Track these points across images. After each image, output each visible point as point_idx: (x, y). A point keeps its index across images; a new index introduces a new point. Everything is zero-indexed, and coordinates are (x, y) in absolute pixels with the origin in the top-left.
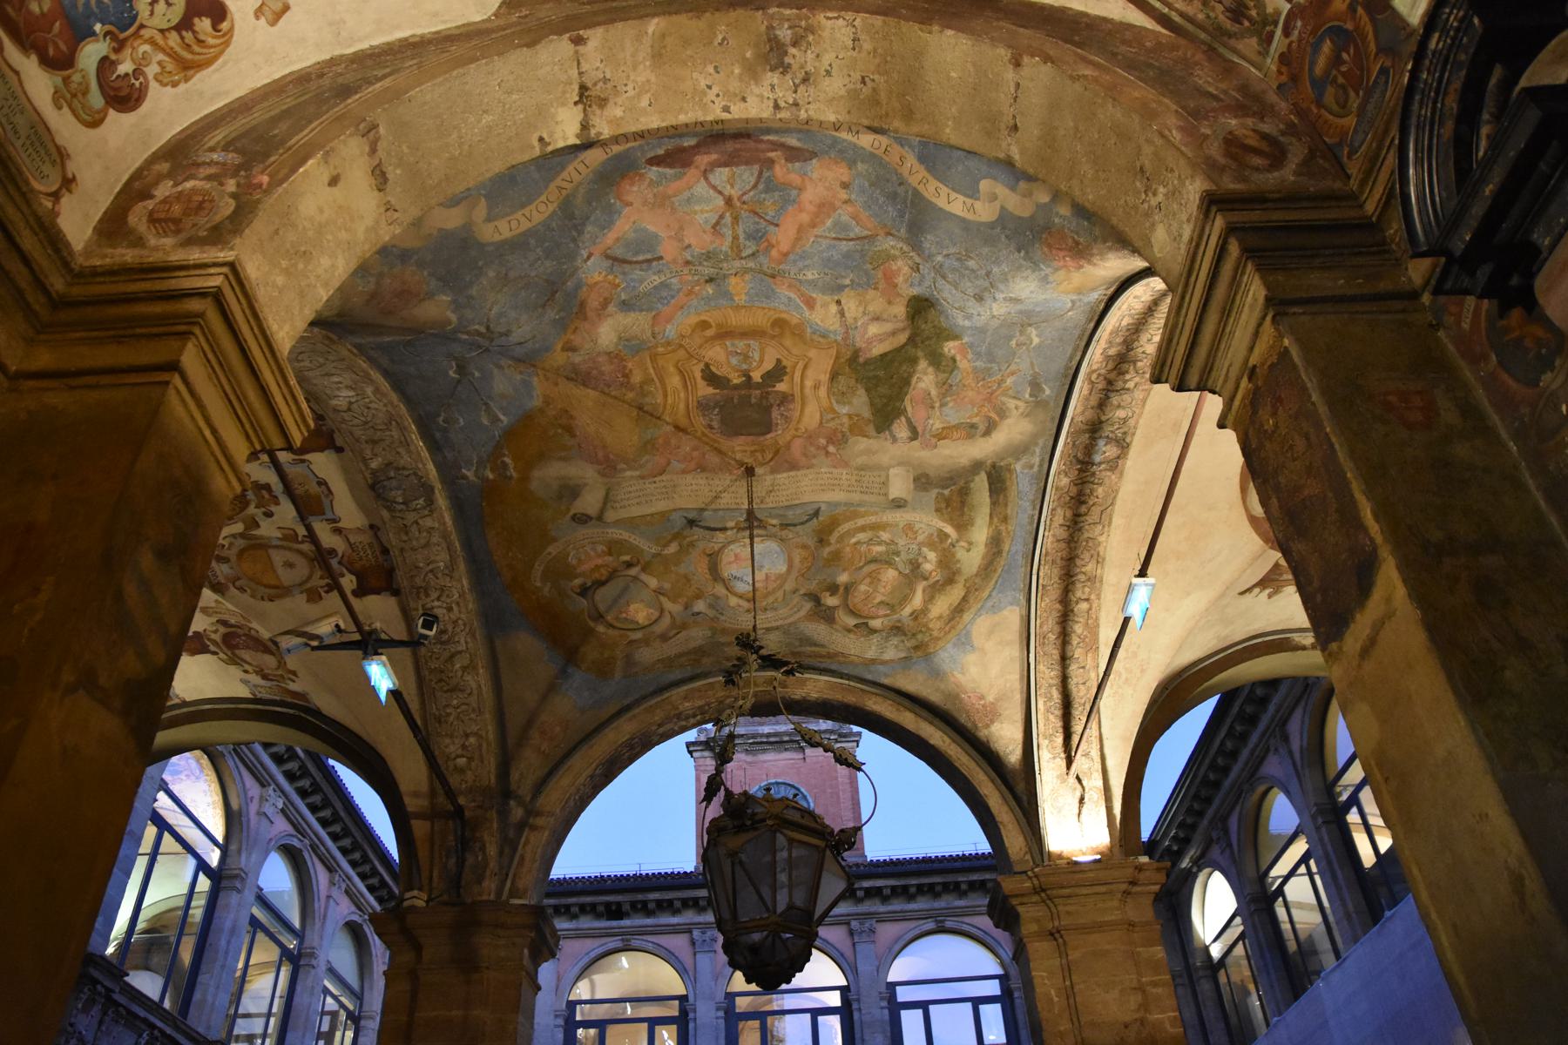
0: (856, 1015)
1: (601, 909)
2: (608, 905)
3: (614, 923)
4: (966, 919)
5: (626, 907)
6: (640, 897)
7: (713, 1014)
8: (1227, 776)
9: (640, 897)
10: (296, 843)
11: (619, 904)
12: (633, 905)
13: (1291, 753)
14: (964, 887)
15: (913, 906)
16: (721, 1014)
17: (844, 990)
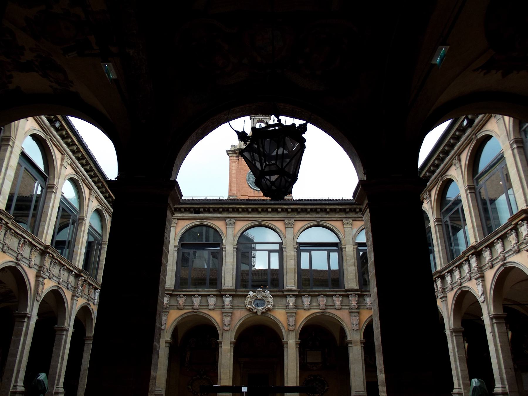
0: (284, 253)
1: (192, 210)
2: (195, 209)
3: (197, 215)
4: (328, 222)
5: (202, 210)
6: (207, 206)
7: (232, 249)
8: (438, 168)
9: (207, 206)
10: (76, 177)
11: (199, 209)
12: (204, 209)
13: (461, 166)
14: (328, 210)
15: (308, 216)
16: (235, 250)
17: (281, 244)
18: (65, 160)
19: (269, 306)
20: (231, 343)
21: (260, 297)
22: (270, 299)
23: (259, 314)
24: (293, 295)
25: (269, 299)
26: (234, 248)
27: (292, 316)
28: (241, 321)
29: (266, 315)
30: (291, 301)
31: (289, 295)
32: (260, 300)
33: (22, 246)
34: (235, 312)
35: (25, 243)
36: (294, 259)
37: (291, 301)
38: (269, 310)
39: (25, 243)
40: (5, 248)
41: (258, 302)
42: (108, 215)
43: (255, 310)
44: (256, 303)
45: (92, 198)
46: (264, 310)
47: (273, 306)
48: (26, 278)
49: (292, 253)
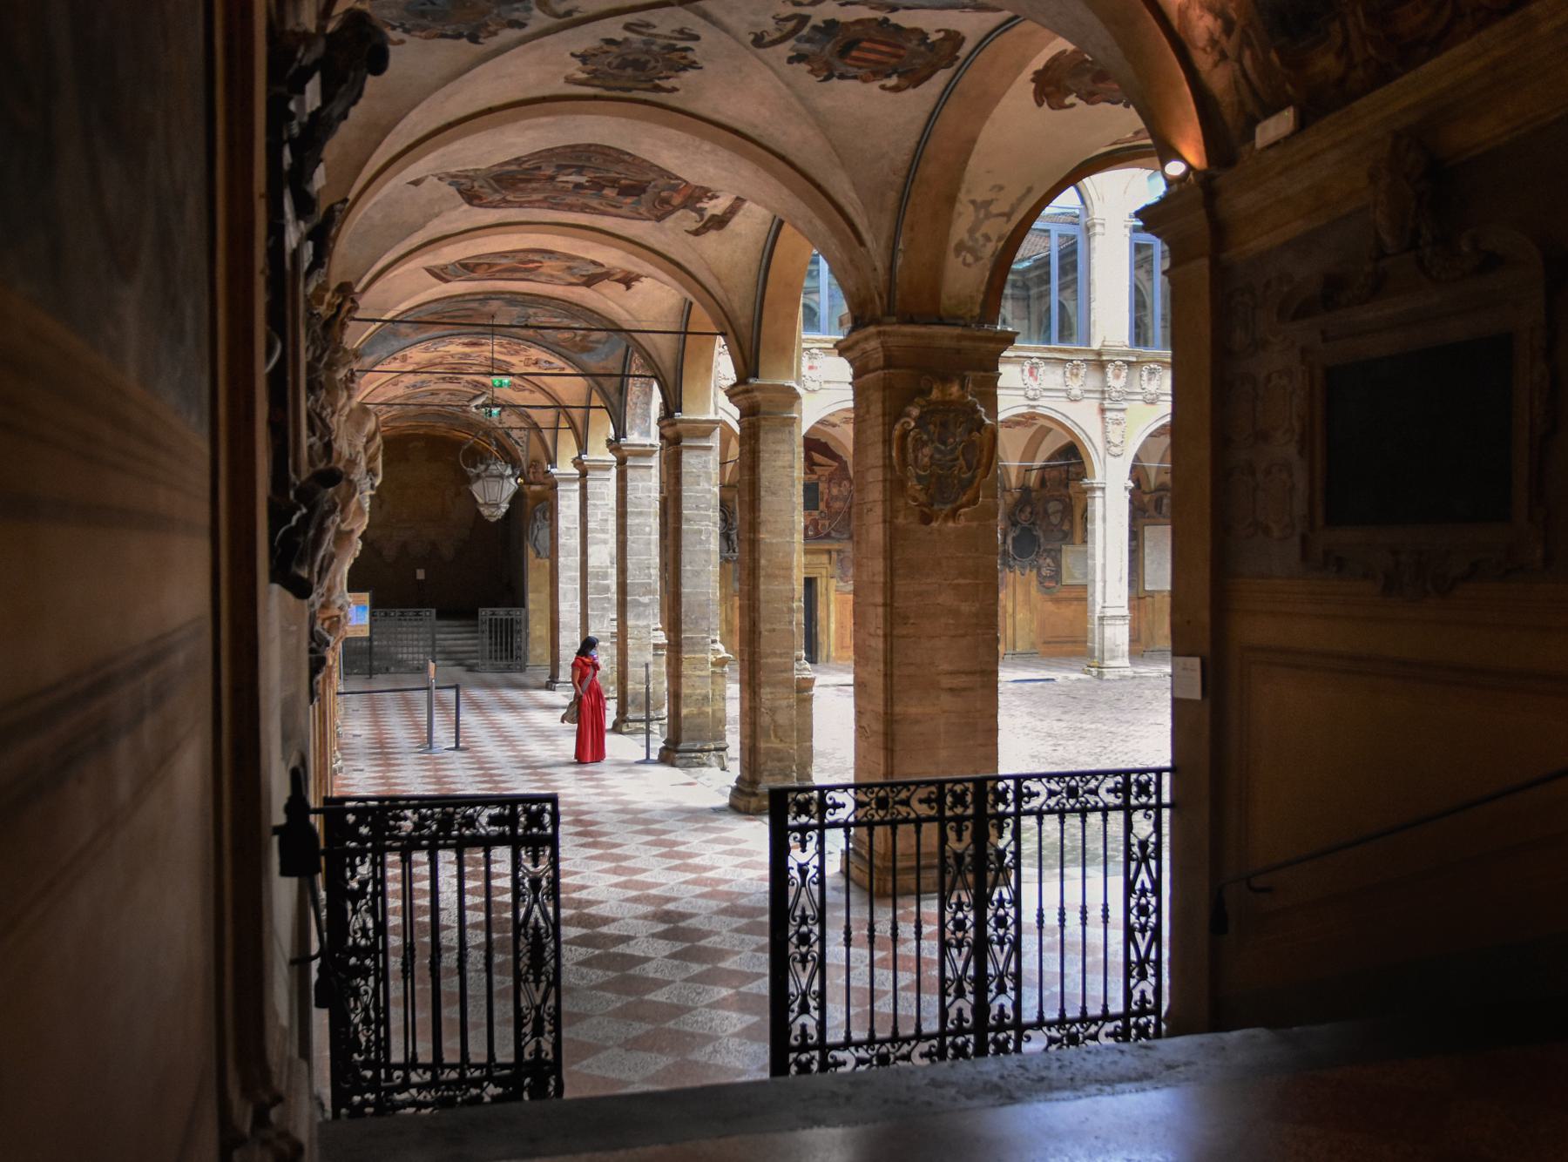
33: (1031, 374)
48: (1068, 423)
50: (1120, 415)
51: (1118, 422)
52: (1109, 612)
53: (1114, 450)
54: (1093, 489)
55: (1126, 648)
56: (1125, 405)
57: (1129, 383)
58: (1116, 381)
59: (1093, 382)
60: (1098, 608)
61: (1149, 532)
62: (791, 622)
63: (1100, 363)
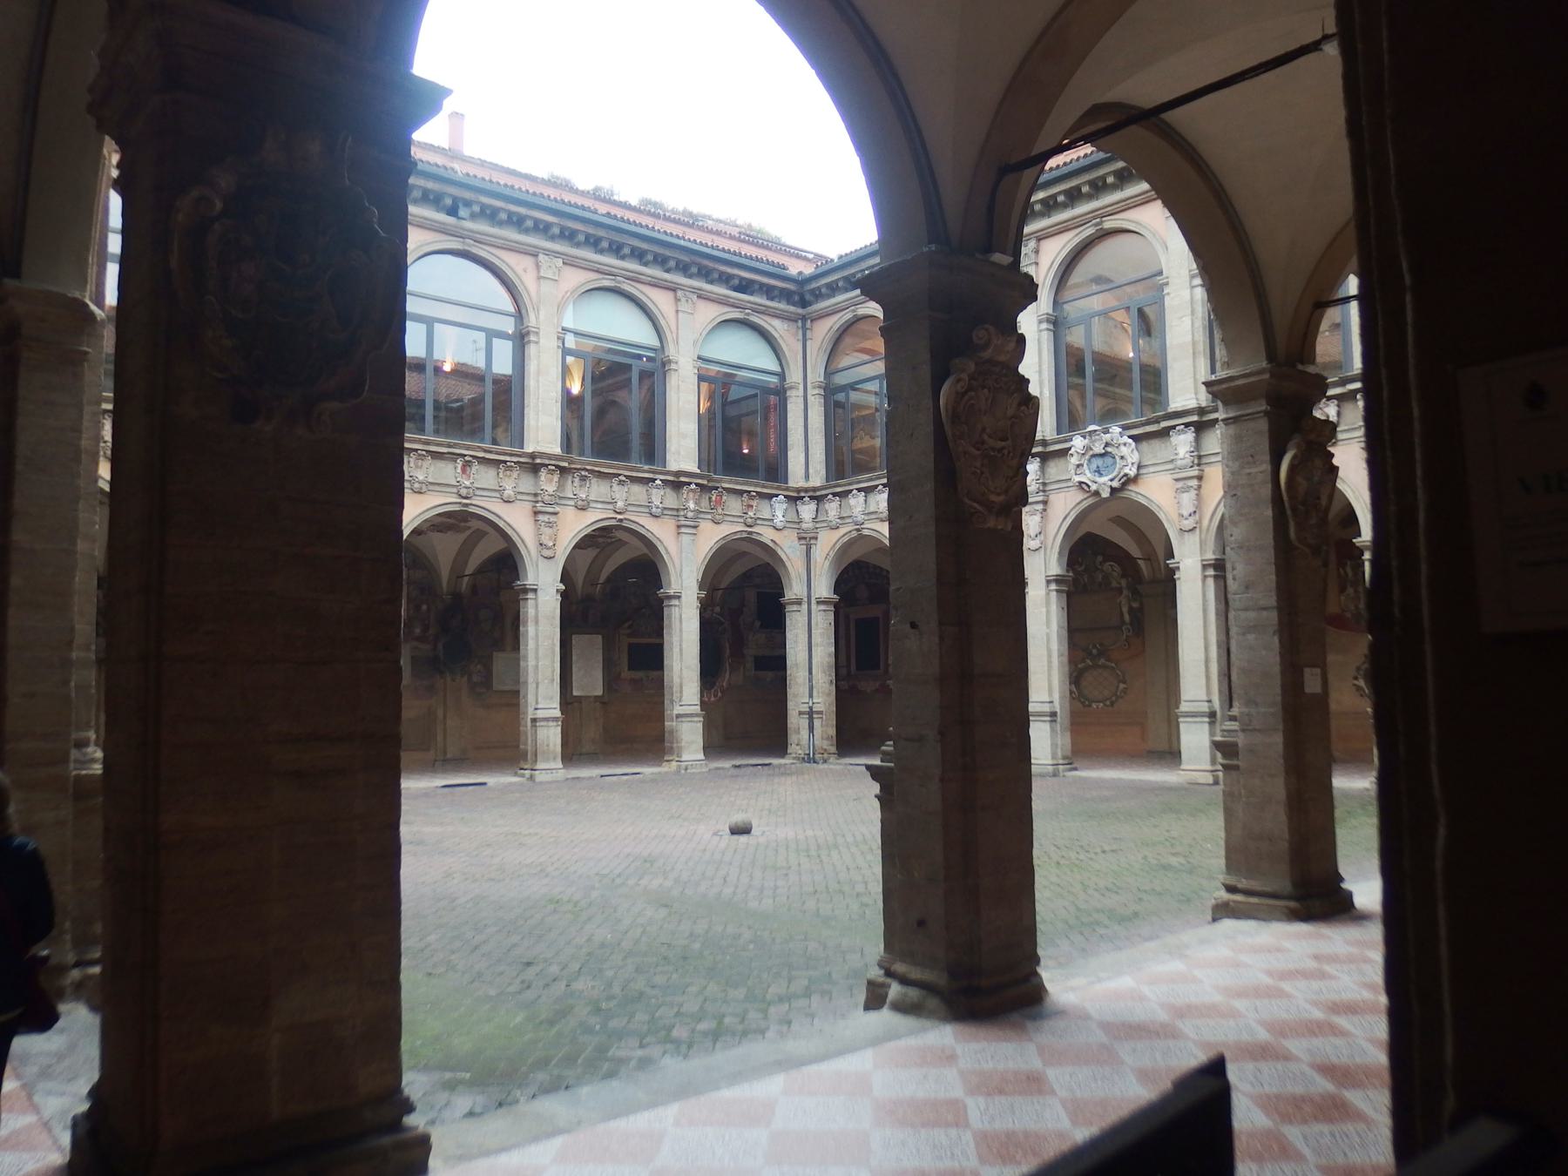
18: (544, 266)
19: (1126, 470)
20: (1048, 582)
21: (1098, 449)
22: (1124, 450)
23: (1105, 494)
24: (1187, 425)
25: (1123, 448)
26: (1040, 322)
27: (1187, 489)
28: (1069, 520)
29: (1125, 494)
30: (1183, 443)
31: (1174, 427)
32: (1102, 455)
33: (464, 471)
34: (1053, 497)
35: (467, 465)
36: (1193, 313)
37: (1183, 443)
38: (1129, 481)
39: (467, 465)
40: (416, 485)
41: (1098, 462)
42: (777, 323)
43: (1094, 487)
44: (1094, 467)
45: (683, 306)
46: (1115, 484)
47: (1139, 467)
48: (501, 524)
49: (1186, 293)
50: (553, 519)
51: (550, 525)
52: (540, 714)
53: (547, 553)
54: (526, 591)
55: (559, 749)
56: (558, 509)
57: (561, 486)
58: (548, 483)
59: (526, 483)
60: (530, 710)
61: (576, 639)
62: (66, 682)
63: (533, 466)
